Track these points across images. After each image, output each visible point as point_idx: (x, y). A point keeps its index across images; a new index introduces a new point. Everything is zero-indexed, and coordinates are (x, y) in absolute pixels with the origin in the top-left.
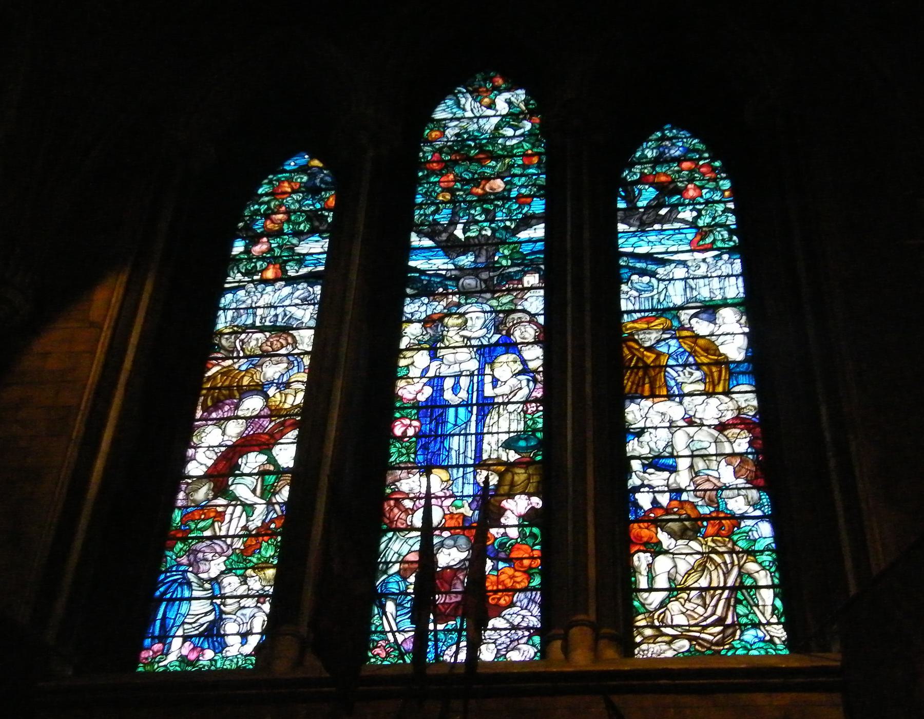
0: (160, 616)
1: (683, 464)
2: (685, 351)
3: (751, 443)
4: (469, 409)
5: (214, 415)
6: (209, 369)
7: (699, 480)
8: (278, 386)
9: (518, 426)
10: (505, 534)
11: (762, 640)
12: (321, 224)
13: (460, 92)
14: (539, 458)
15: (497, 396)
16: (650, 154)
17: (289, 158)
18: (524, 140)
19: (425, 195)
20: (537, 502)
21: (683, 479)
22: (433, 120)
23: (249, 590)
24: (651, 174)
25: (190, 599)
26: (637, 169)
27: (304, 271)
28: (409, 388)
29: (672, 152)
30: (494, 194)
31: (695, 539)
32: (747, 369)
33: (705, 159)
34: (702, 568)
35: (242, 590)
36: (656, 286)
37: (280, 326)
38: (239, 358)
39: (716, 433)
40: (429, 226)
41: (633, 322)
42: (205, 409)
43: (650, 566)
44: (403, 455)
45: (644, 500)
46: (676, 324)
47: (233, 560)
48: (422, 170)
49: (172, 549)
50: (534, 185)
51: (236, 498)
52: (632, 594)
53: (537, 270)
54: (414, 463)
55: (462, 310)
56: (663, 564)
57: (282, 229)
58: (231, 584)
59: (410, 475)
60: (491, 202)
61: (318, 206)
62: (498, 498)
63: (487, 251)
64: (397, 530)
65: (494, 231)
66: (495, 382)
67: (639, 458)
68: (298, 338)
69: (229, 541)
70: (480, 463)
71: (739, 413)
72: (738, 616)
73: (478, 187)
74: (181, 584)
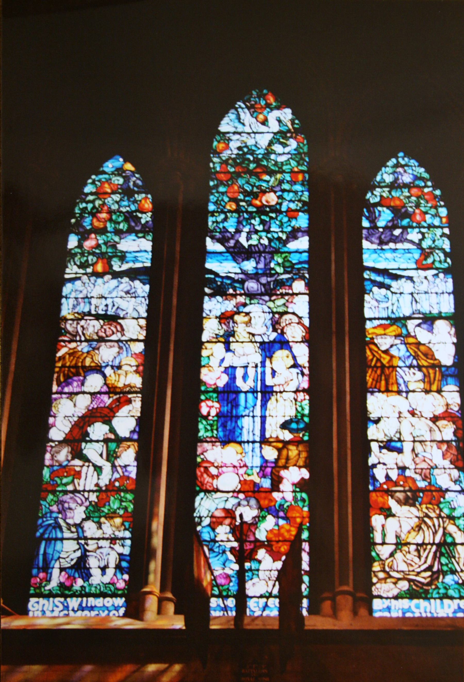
0: (42, 551)
2: (411, 355)
3: (455, 433)
4: (255, 395)
5: (66, 390)
7: (417, 460)
8: (112, 367)
10: (283, 498)
12: (136, 225)
13: (240, 107)
14: (306, 438)
15: (275, 385)
17: (106, 160)
18: (291, 158)
19: (216, 203)
20: (305, 474)
22: (219, 133)
23: (104, 533)
24: (388, 197)
25: (62, 539)
26: (378, 191)
27: (125, 267)
28: (211, 374)
29: (404, 178)
30: (270, 207)
31: (413, 505)
32: (454, 373)
33: (428, 187)
35: (99, 534)
36: (390, 298)
37: (111, 315)
38: (81, 341)
39: (431, 424)
40: (220, 232)
41: (375, 328)
42: (59, 384)
44: (208, 430)
46: (404, 332)
47: (91, 510)
48: (213, 180)
49: (45, 500)
50: (299, 201)
51: (88, 460)
52: (371, 546)
54: (216, 438)
55: (246, 310)
57: (105, 228)
59: (214, 447)
60: (266, 214)
61: (133, 208)
62: (277, 469)
63: (265, 257)
64: (207, 491)
65: (270, 240)
67: (377, 441)
68: (125, 327)
69: (86, 494)
70: (264, 441)
71: (447, 408)
72: (442, 565)
73: (256, 199)
74: (54, 528)
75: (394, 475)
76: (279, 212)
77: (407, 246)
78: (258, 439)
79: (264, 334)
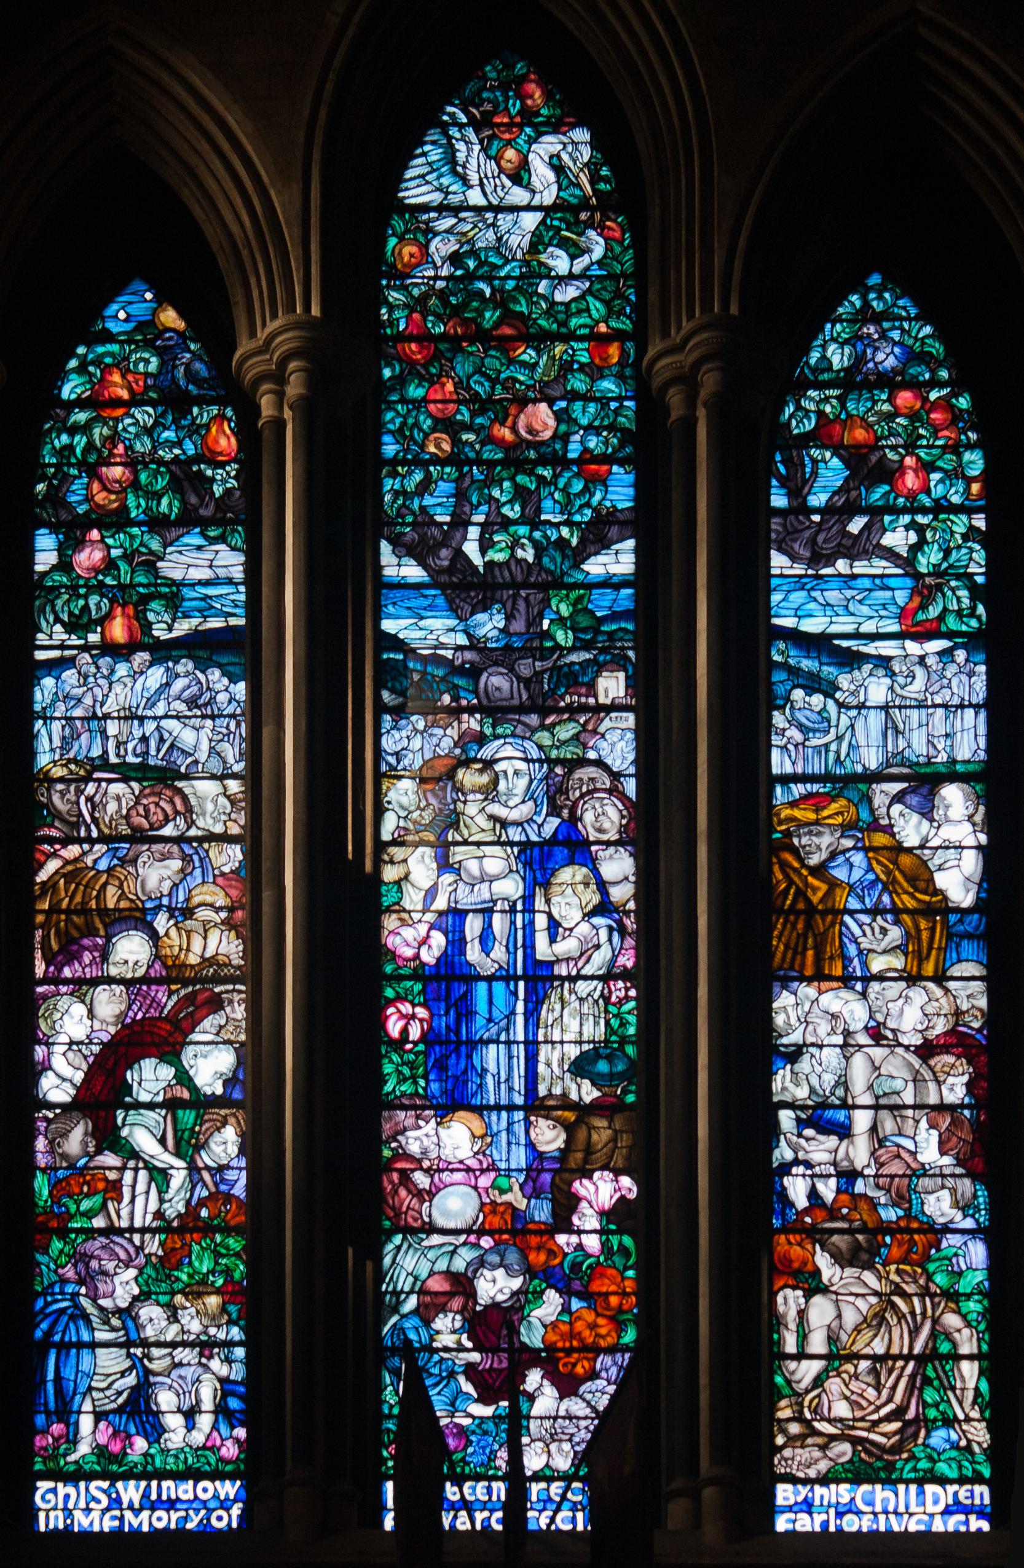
1: (862, 1120)
6: (41, 866)
8: (171, 911)
9: (594, 1030)
11: (955, 1446)
16: (838, 358)
21: (860, 1153)
27: (183, 627)
28: (408, 933)
34: (876, 1321)
43: (802, 1314)
45: (797, 1189)
53: (620, 662)
55: (486, 752)
56: (821, 1311)
58: (151, 1314)
66: (554, 925)
70: (535, 1105)
75: (828, 1190)
76: (560, 462)
77: (880, 566)
78: (519, 1100)
79: (530, 821)
